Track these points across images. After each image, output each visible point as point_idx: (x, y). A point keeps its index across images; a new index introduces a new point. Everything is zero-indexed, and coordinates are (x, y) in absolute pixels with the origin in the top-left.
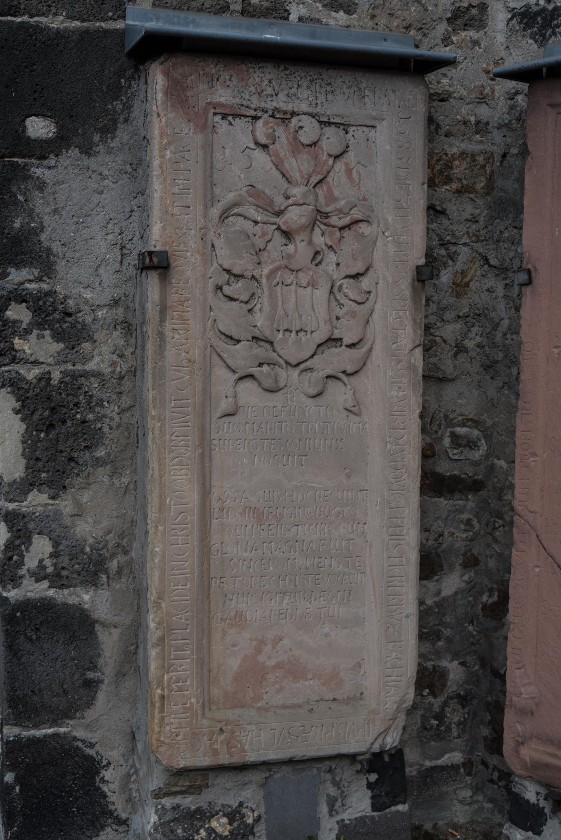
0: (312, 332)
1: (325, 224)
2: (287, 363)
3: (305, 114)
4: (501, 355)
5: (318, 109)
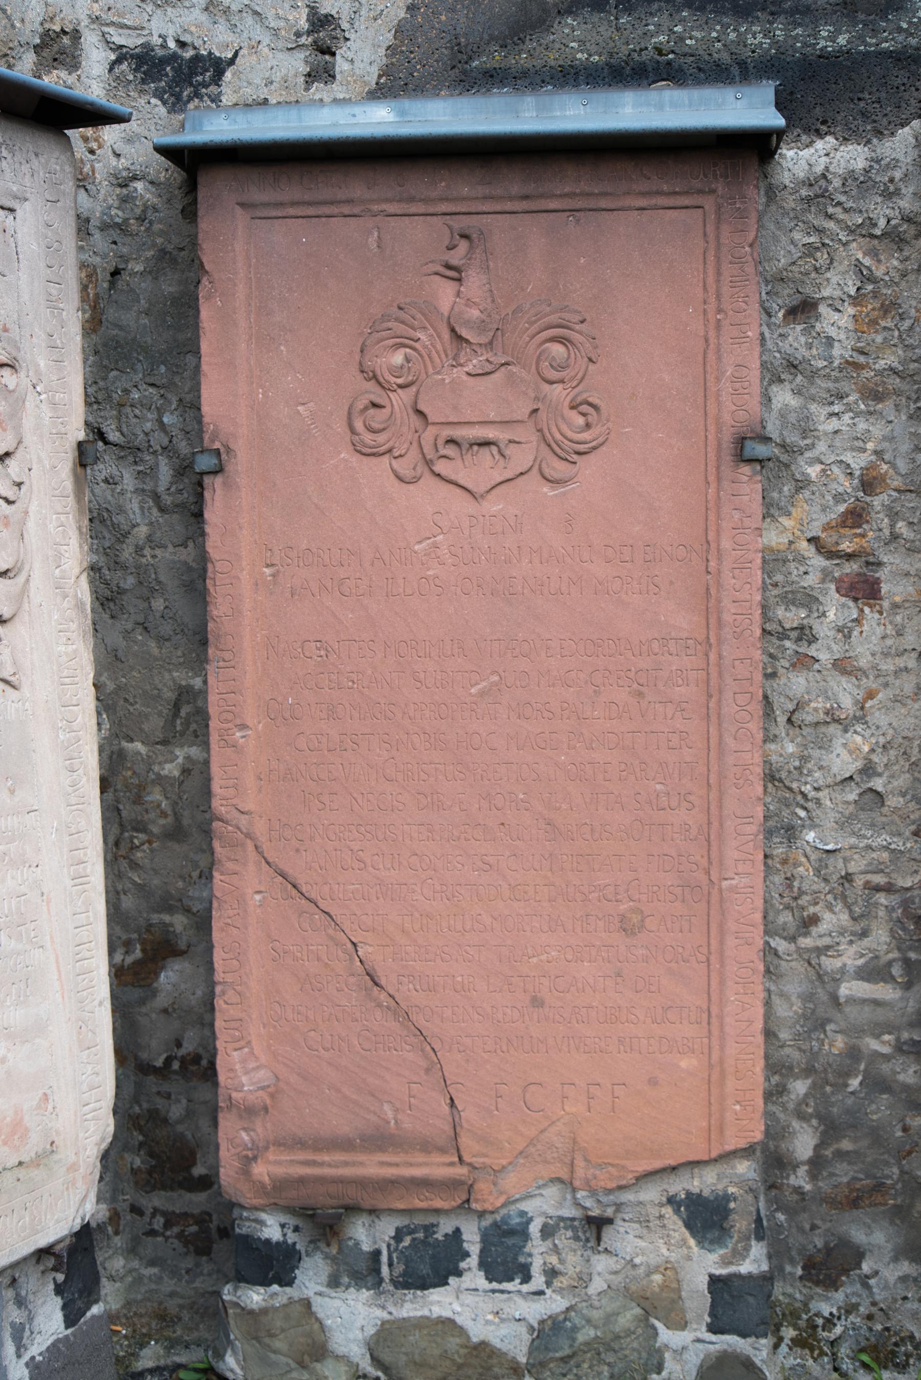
4: (130, 581)
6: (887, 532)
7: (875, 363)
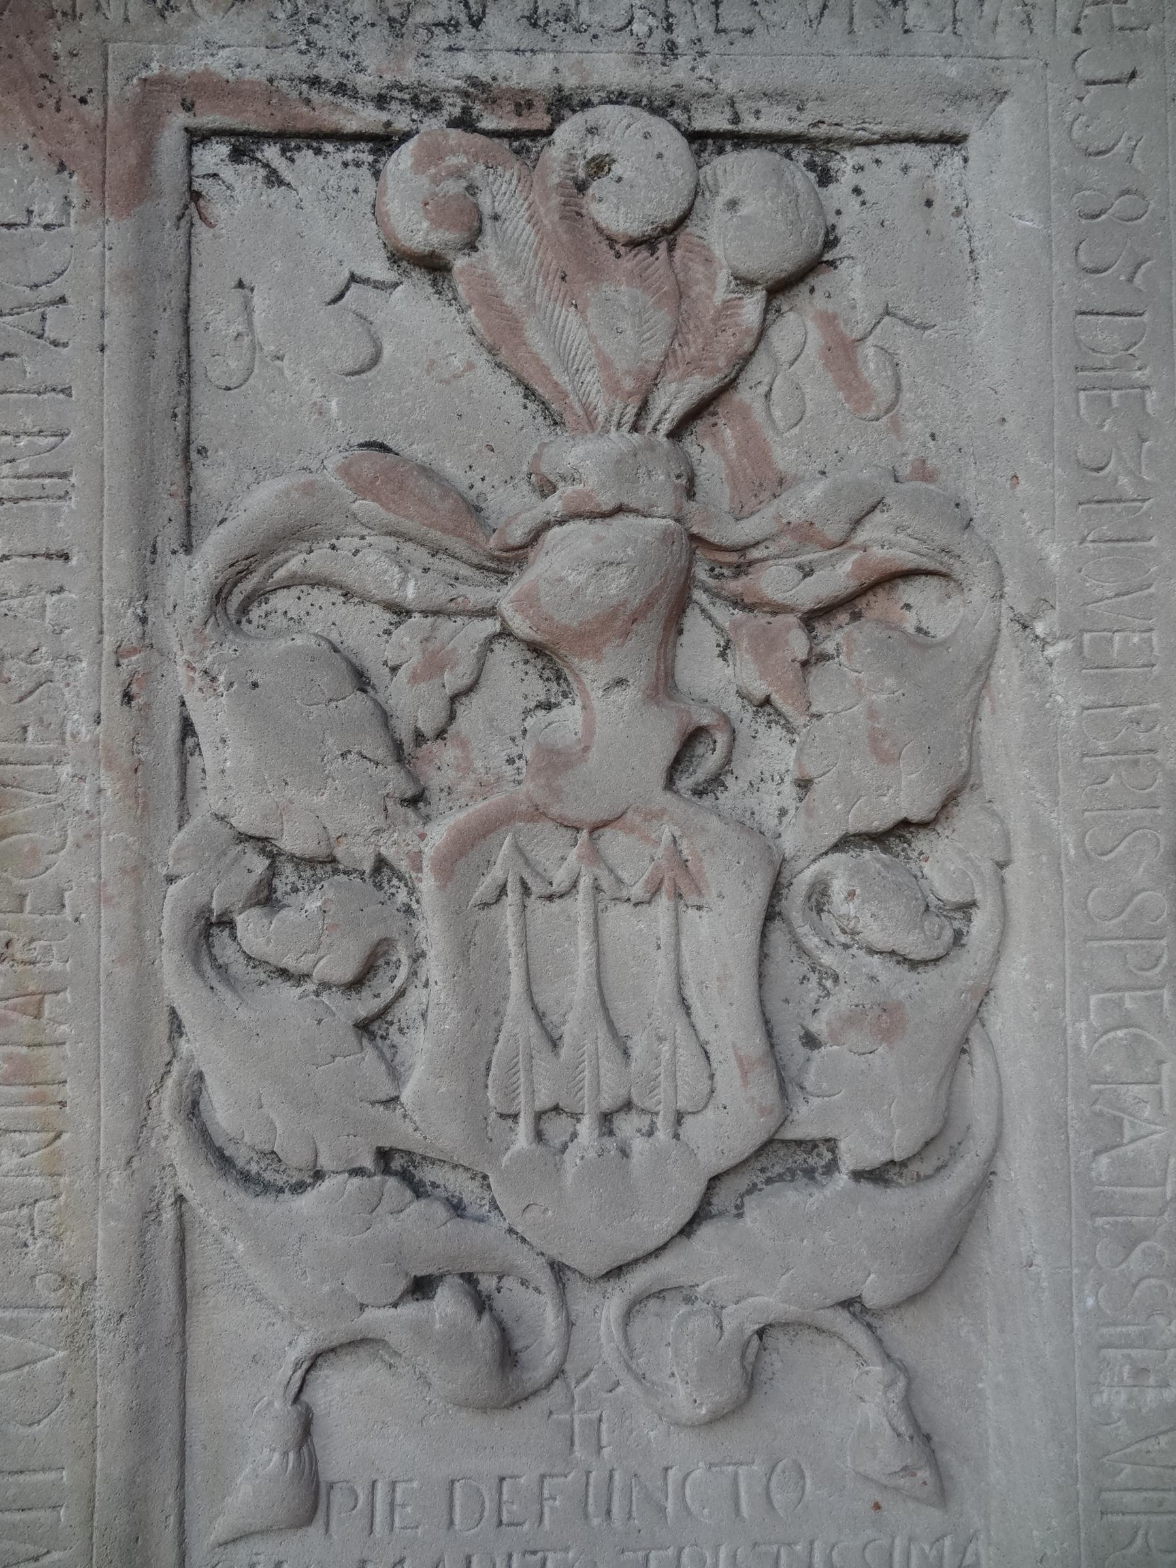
0: (679, 1117)
1: (737, 602)
2: (558, 1269)
3: (618, 98)
5: (680, 71)
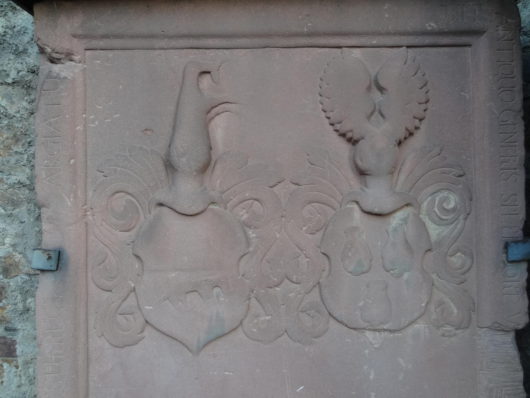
6: (20, 306)
7: (8, 179)
